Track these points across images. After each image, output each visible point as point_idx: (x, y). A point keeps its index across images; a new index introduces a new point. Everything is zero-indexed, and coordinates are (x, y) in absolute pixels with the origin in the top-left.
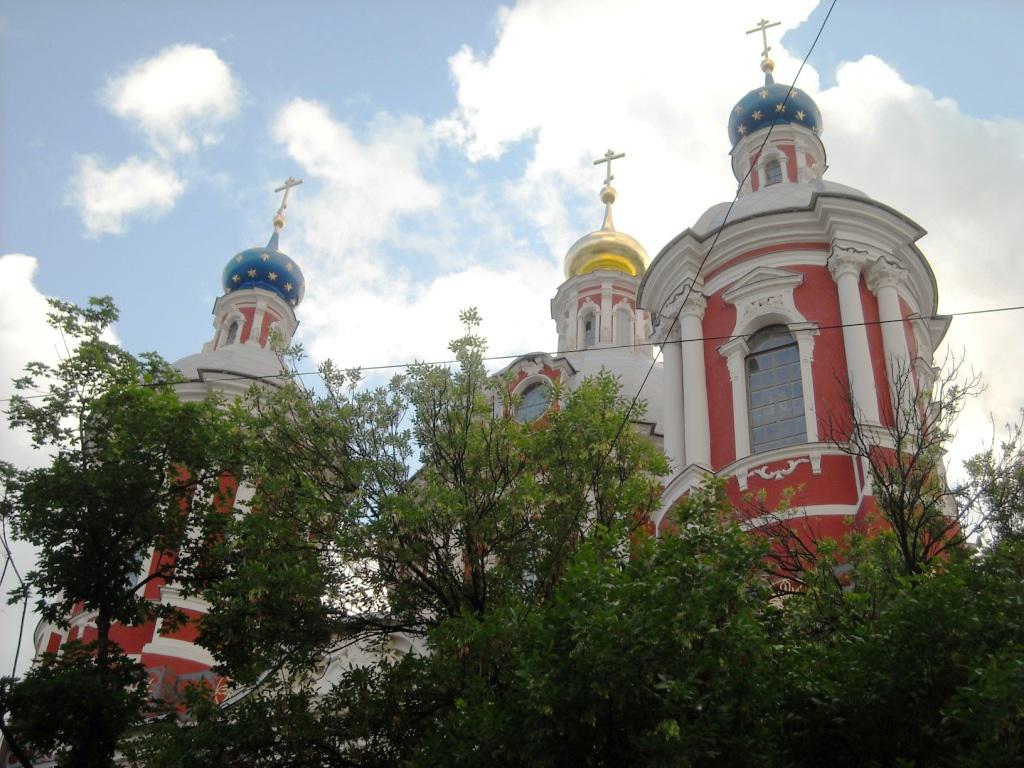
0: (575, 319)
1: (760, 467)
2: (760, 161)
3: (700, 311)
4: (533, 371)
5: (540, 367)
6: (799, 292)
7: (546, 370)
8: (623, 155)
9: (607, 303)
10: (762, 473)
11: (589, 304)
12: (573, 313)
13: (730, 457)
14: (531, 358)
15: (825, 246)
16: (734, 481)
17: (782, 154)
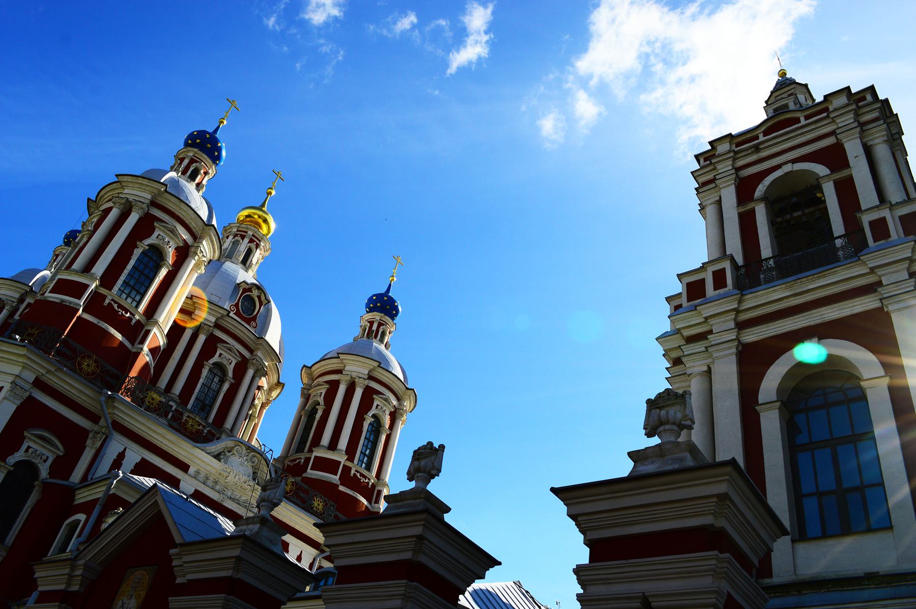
4: (255, 293)
7: (259, 297)
12: (246, 240)
16: (350, 469)
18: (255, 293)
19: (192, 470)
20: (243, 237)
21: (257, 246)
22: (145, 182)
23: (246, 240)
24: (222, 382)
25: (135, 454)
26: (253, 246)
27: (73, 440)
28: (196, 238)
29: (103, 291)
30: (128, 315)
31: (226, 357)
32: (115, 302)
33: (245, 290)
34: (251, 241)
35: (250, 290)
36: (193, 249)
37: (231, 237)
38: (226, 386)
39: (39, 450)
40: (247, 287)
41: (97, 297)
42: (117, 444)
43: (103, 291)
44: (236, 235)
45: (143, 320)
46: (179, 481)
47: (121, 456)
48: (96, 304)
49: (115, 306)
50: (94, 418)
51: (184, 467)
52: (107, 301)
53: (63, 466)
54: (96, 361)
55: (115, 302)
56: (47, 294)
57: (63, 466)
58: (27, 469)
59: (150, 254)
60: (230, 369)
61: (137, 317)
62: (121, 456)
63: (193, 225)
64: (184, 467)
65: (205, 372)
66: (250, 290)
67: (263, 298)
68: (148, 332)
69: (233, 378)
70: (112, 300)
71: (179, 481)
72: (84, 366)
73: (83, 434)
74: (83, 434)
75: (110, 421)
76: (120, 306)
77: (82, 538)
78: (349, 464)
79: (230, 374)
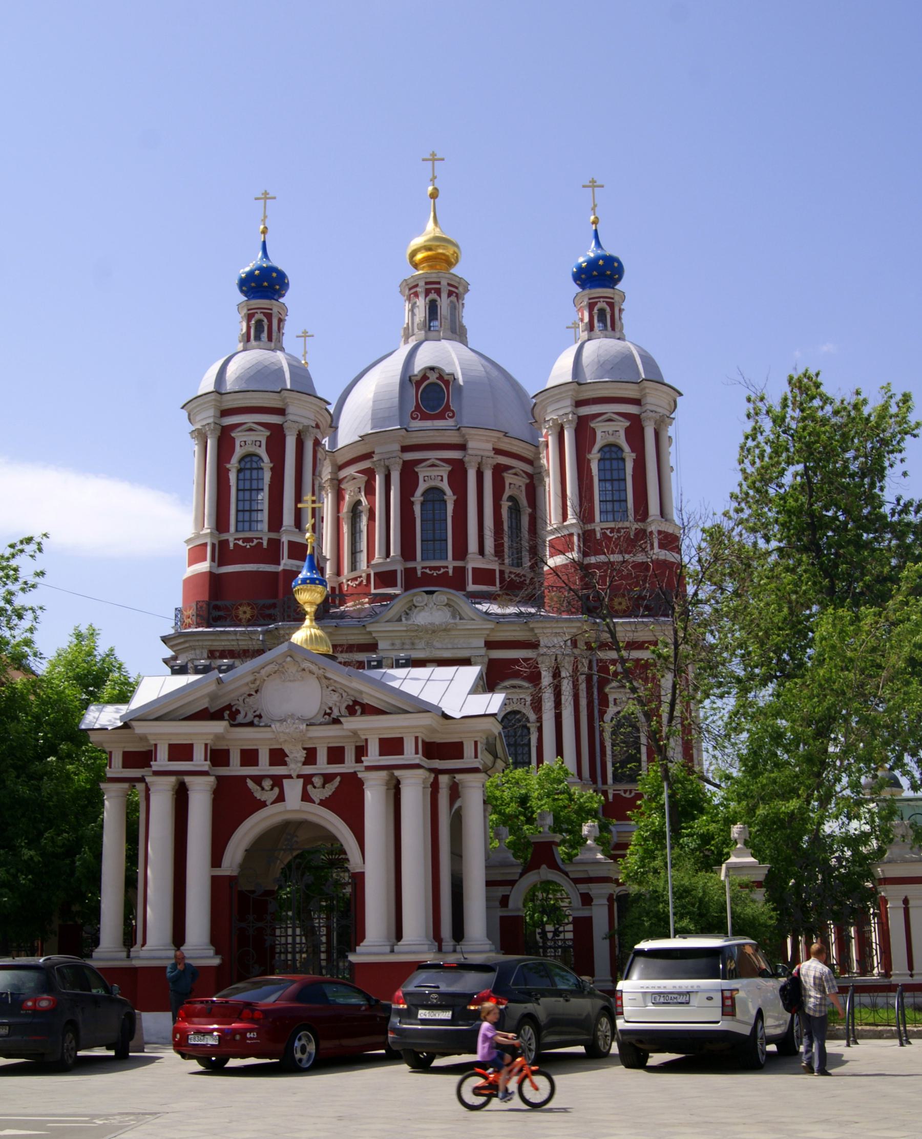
0: (421, 302)
1: (607, 529)
2: (596, 311)
3: (574, 425)
4: (433, 377)
5: (437, 375)
6: (627, 431)
7: (441, 378)
8: (443, 160)
9: (444, 295)
10: (608, 532)
11: (433, 296)
13: (592, 520)
14: (432, 369)
15: (637, 402)
17: (608, 309)
26: (433, 296)
30: (255, 541)
31: (432, 476)
32: (238, 539)
33: (418, 384)
34: (427, 292)
35: (425, 378)
40: (419, 378)
49: (240, 543)
52: (231, 545)
54: (249, 605)
55: (238, 539)
60: (445, 486)
65: (417, 509)
69: (454, 494)
70: (236, 539)
72: (241, 616)
76: (246, 540)
78: (589, 527)
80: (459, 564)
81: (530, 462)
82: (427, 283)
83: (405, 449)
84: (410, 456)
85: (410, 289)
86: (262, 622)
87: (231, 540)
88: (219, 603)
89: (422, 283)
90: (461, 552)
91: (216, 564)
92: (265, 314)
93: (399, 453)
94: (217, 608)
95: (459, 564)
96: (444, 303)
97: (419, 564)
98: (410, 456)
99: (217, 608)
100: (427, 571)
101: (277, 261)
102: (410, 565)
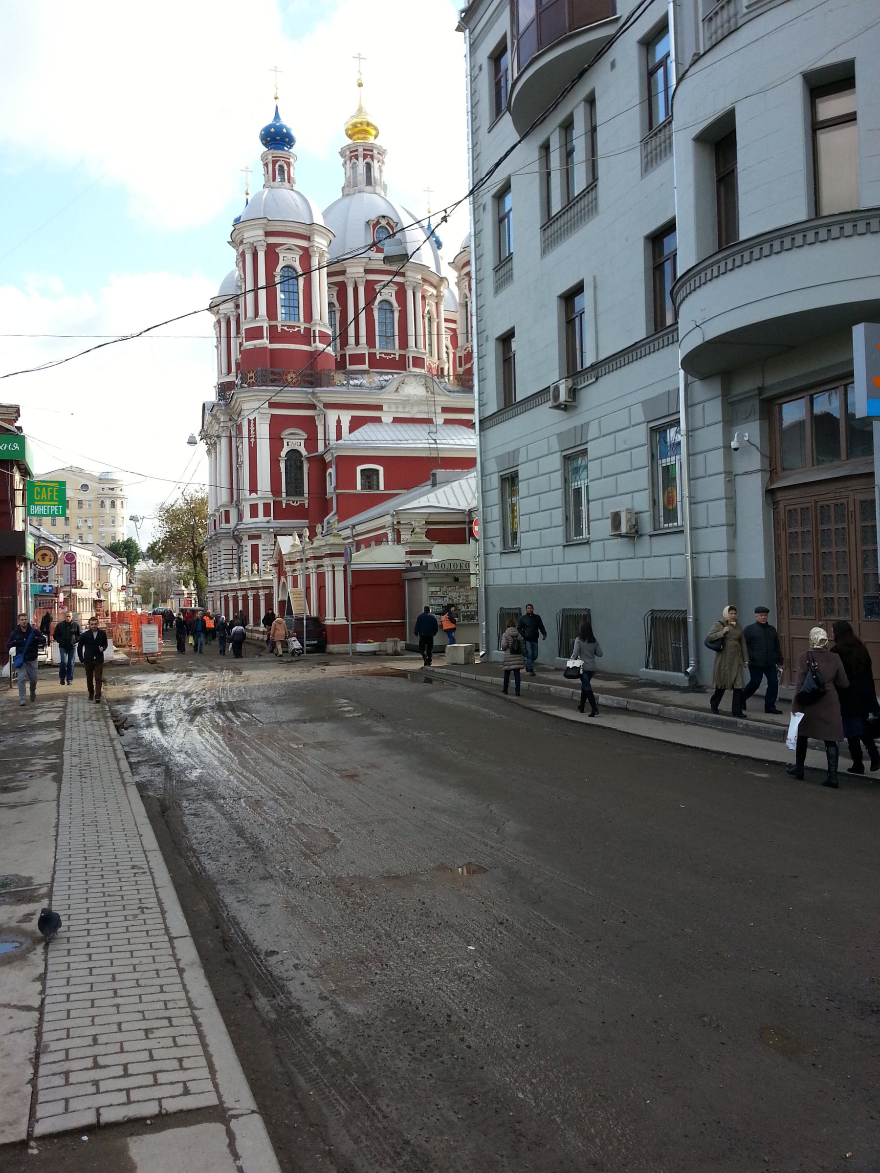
0: (361, 164)
4: (383, 222)
7: (388, 224)
9: (376, 161)
12: (361, 159)
14: (384, 217)
18: (383, 222)
19: (385, 408)
20: (356, 157)
21: (372, 157)
22: (252, 223)
23: (361, 159)
24: (392, 312)
25: (346, 417)
26: (368, 160)
27: (309, 425)
28: (308, 238)
29: (273, 323)
30: (297, 329)
33: (374, 226)
34: (365, 156)
35: (378, 222)
36: (310, 250)
37: (348, 162)
38: (396, 315)
39: (294, 441)
41: (273, 328)
42: (332, 416)
43: (273, 323)
44: (351, 159)
45: (307, 326)
46: (380, 418)
47: (339, 421)
48: (275, 335)
49: (286, 328)
50: (313, 407)
51: (379, 408)
53: (311, 443)
56: (245, 344)
57: (311, 443)
58: (294, 454)
59: (286, 274)
61: (303, 327)
62: (339, 421)
63: (301, 231)
64: (379, 408)
65: (376, 313)
66: (378, 222)
67: (392, 223)
68: (314, 331)
71: (380, 418)
73: (312, 419)
74: (312, 419)
75: (321, 406)
76: (289, 327)
77: (333, 485)
79: (395, 304)
80: (403, 352)
81: (435, 287)
82: (364, 150)
83: (367, 271)
84: (371, 277)
85: (351, 152)
86: (303, 385)
87: (279, 325)
88: (273, 370)
89: (361, 149)
90: (404, 344)
91: (268, 342)
92: (286, 162)
93: (363, 275)
94: (273, 373)
95: (403, 352)
96: (375, 165)
97: (378, 350)
98: (371, 277)
99: (273, 373)
100: (383, 355)
101: (288, 121)
102: (372, 351)
